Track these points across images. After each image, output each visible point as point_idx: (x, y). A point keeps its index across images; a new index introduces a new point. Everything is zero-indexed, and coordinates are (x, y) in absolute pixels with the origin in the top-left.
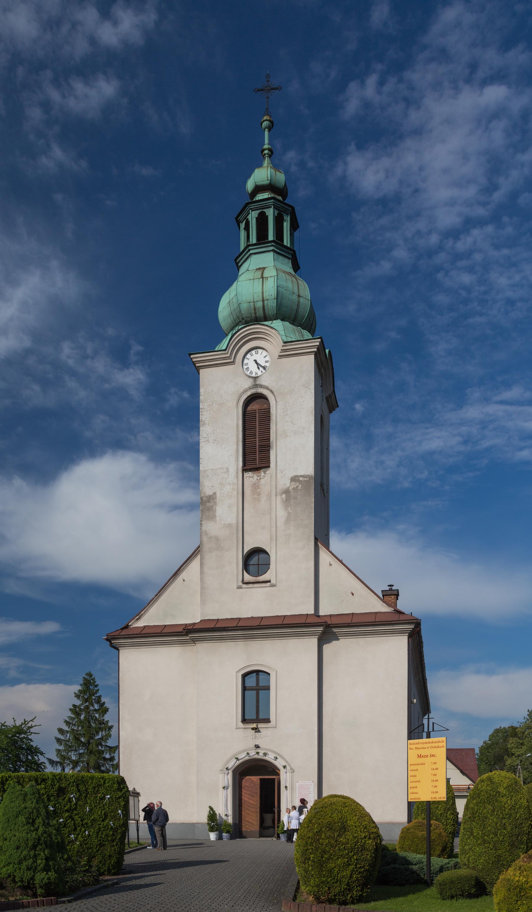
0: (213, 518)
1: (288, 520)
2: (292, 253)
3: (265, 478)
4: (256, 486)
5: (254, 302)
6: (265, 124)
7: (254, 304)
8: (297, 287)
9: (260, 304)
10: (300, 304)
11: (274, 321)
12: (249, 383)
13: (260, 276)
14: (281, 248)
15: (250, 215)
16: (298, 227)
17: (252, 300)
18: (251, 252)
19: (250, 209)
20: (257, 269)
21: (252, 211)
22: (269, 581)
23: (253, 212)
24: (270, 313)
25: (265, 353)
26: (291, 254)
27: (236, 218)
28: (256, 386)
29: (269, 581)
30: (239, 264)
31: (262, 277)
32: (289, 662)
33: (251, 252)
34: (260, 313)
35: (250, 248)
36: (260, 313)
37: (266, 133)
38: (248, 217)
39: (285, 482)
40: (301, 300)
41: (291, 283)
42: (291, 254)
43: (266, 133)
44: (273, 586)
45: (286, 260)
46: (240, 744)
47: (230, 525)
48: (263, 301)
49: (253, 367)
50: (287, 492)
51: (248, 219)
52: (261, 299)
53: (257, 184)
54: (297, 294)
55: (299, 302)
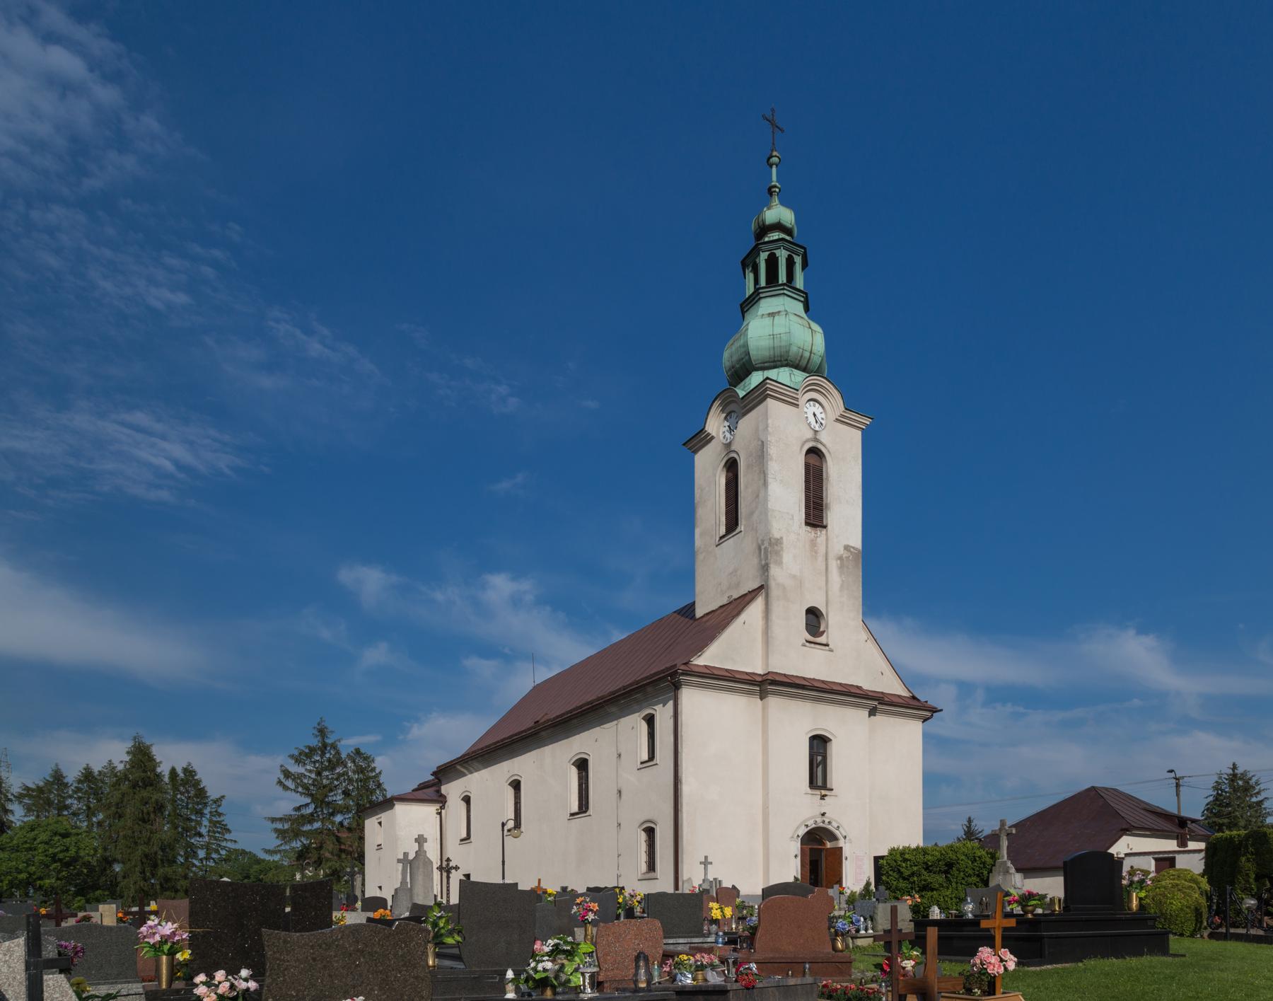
0: (780, 563)
1: (842, 586)
3: (821, 534)
4: (813, 543)
6: (775, 160)
9: (807, 354)
12: (810, 435)
22: (827, 645)
25: (821, 410)
28: (816, 440)
29: (827, 645)
32: (848, 729)
34: (804, 363)
36: (804, 363)
37: (774, 169)
39: (837, 549)
43: (774, 169)
44: (831, 651)
46: (803, 810)
47: (794, 577)
49: (812, 419)
50: (840, 558)
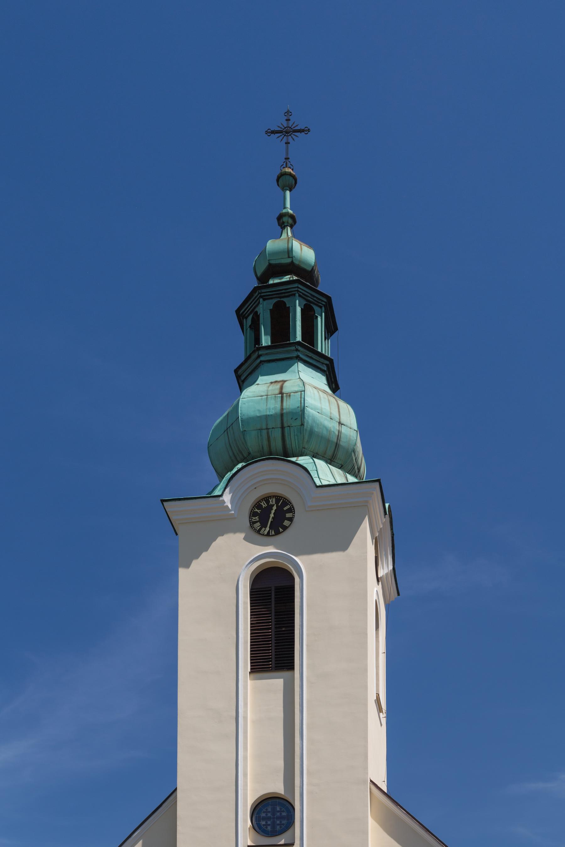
2: (328, 362)
5: (267, 429)
7: (268, 433)
8: (337, 410)
10: (342, 436)
11: (300, 458)
13: (277, 392)
14: (311, 354)
15: (261, 306)
16: (336, 329)
17: (264, 427)
18: (262, 358)
19: (261, 297)
20: (271, 383)
21: (264, 300)
23: (265, 302)
24: (294, 446)
26: (326, 364)
27: (238, 311)
30: (243, 378)
31: (281, 393)
33: (262, 358)
35: (260, 353)
38: (257, 309)
40: (344, 430)
41: (328, 404)
42: (326, 364)
45: (319, 375)
48: (283, 428)
51: (257, 312)
52: (279, 425)
53: (272, 262)
54: (338, 421)
55: (339, 432)
